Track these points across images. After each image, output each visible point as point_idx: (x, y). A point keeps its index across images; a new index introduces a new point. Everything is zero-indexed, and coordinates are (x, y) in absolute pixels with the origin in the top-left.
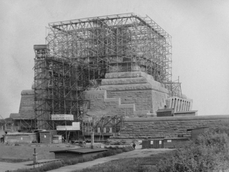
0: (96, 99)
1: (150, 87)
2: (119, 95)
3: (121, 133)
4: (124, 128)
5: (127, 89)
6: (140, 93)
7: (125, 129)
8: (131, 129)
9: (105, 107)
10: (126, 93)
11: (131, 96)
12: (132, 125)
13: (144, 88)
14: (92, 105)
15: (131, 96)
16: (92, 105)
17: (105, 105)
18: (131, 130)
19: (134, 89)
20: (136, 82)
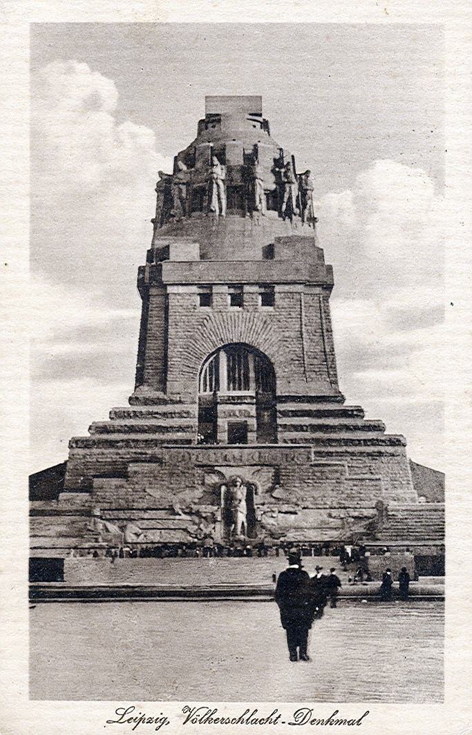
14: (283, 476)
16: (283, 476)
18: (404, 529)
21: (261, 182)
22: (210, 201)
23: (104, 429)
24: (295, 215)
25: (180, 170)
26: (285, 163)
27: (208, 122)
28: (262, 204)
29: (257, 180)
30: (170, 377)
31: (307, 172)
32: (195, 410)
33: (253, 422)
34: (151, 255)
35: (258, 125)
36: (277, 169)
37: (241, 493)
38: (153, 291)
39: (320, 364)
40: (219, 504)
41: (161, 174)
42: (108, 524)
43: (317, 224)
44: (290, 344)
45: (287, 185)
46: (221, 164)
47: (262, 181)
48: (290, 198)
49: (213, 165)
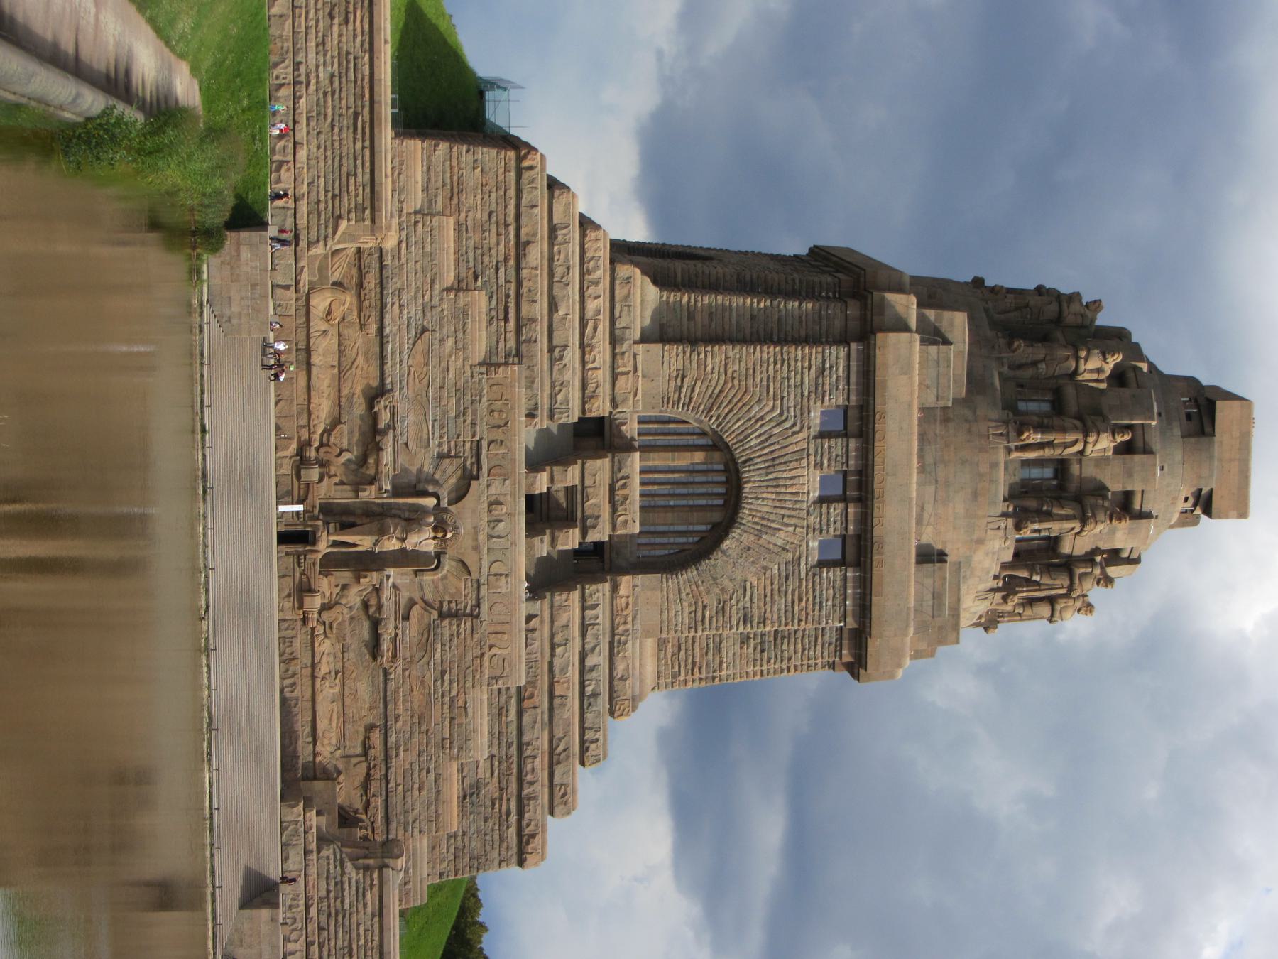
0: (486, 648)
1: (530, 859)
2: (500, 714)
3: (328, 858)
4: (353, 875)
6: (508, 813)
7: (350, 879)
8: (347, 907)
9: (447, 699)
10: (509, 745)
11: (492, 774)
12: (365, 906)
13: (527, 831)
14: (458, 626)
15: (496, 773)
17: (454, 693)
19: (525, 785)
20: (558, 771)
21: (1077, 530)
22: (1041, 428)
24: (1005, 599)
25: (1105, 359)
26: (1112, 571)
29: (1077, 525)
30: (673, 351)
31: (1089, 608)
32: (601, 408)
33: (570, 540)
35: (1188, 506)
36: (1098, 559)
37: (423, 540)
38: (853, 310)
39: (694, 663)
41: (1096, 305)
43: (981, 629)
44: (738, 601)
45: (1066, 583)
46: (1115, 447)
47: (1078, 534)
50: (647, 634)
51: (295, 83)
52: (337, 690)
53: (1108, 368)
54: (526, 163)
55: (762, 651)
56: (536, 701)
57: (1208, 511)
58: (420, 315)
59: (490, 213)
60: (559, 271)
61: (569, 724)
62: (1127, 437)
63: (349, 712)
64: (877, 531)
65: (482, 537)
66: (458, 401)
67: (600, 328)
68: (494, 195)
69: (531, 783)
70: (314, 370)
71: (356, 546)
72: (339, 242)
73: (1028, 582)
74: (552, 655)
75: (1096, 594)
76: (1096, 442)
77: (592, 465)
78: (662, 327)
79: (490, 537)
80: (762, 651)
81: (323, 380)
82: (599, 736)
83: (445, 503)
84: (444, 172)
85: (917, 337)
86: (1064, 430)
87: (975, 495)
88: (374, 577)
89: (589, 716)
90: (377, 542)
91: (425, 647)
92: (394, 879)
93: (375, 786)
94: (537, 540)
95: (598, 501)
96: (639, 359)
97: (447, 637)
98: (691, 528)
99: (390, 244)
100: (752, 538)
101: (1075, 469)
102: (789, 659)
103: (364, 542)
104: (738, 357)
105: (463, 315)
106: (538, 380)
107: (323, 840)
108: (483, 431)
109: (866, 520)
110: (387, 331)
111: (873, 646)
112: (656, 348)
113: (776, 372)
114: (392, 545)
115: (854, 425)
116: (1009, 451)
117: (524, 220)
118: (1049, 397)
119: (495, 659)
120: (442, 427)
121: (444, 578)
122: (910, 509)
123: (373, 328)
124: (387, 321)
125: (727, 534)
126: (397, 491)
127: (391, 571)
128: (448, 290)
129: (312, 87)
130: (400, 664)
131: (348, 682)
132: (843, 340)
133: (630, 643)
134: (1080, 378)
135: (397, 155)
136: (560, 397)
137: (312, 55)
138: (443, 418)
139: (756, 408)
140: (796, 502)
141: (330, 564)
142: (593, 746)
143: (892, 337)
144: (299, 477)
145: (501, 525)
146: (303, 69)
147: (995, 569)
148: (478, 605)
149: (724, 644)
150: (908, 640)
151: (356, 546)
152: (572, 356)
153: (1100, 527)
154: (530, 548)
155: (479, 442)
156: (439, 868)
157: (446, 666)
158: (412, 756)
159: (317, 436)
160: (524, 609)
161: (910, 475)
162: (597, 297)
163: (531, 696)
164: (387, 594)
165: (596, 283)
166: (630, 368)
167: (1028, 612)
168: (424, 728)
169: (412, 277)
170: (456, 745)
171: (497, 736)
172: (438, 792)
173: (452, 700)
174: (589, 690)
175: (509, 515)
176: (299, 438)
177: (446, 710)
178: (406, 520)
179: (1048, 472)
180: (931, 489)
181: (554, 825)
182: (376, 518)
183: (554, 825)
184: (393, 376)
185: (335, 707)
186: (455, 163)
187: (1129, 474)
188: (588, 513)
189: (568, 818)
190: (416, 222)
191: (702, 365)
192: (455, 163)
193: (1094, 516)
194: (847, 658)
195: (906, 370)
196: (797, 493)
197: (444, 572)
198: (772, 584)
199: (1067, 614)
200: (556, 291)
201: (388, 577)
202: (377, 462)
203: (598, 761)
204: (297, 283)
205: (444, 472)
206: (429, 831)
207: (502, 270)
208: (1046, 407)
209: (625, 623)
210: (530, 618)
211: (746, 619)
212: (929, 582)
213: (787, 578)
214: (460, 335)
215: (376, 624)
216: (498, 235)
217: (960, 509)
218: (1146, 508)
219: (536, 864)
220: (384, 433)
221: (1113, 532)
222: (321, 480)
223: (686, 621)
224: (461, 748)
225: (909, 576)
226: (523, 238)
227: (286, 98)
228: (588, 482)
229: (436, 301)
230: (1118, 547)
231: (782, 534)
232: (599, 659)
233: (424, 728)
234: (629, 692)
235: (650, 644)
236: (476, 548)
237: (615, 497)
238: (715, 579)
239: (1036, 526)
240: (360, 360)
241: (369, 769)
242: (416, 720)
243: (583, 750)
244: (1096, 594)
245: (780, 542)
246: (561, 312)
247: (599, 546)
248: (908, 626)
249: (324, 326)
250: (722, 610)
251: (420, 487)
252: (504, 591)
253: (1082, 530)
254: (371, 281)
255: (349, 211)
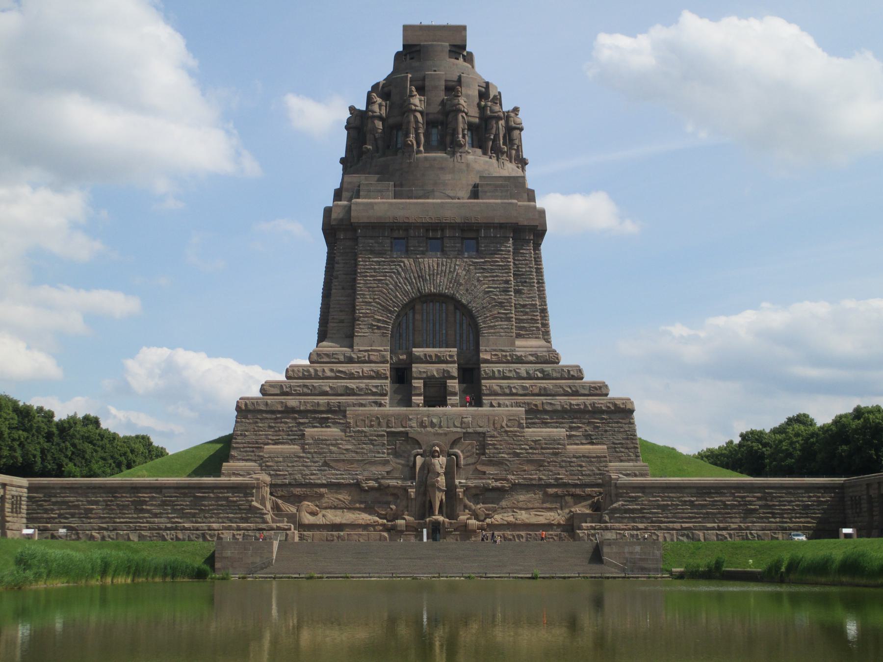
4: (620, 503)
5: (568, 407)
8: (639, 507)
11: (580, 427)
17: (527, 447)
20: (582, 391)
21: (464, 115)
22: (407, 135)
23: (281, 390)
26: (491, 97)
27: (406, 55)
28: (464, 137)
31: (516, 110)
32: (385, 368)
33: (454, 385)
34: (338, 195)
35: (461, 59)
36: (483, 103)
40: (415, 479)
42: (280, 501)
44: (496, 295)
47: (466, 114)
48: (497, 135)
49: (412, 96)
50: (513, 344)
51: (176, 529)
52: (523, 512)
53: (379, 100)
54: (243, 407)
55: (525, 282)
56: (538, 403)
57: (464, 47)
58: (317, 464)
59: (270, 427)
60: (305, 390)
61: (556, 386)
62: (413, 88)
63: (537, 505)
64: (458, 221)
65: (440, 431)
66: (364, 444)
67: (341, 369)
68: (260, 425)
69: (585, 405)
70: (344, 521)
71: (442, 500)
72: (265, 507)
73: (494, 141)
74: (516, 394)
75: (507, 106)
76: (416, 106)
77: (414, 375)
78: (347, 337)
79: (440, 427)
80: (525, 282)
81: (349, 517)
82: (565, 369)
83: (420, 451)
84: (246, 451)
85: (354, 201)
86: (409, 122)
87: (442, 169)
88: (460, 491)
89: (555, 375)
90: (440, 490)
91: (499, 463)
92: (625, 479)
93: (578, 491)
94: (449, 402)
95: (434, 369)
96: (362, 348)
97: (496, 451)
98: (458, 321)
99: (268, 479)
100: (461, 288)
101: (431, 117)
102: (530, 267)
103: (440, 497)
104: (364, 295)
105: (318, 441)
106: (361, 401)
107: (601, 521)
108: (382, 430)
109: (453, 226)
110: (324, 482)
111: (523, 222)
112: (356, 340)
113: (371, 276)
114: (442, 480)
115: (401, 233)
116: (419, 152)
117: (274, 408)
118: (395, 132)
119: (509, 424)
120: (379, 453)
121: (462, 451)
122: (446, 203)
123: (323, 490)
124: (319, 482)
125: (459, 302)
126: (413, 478)
127: (457, 482)
128: (303, 449)
129: (179, 520)
130: (509, 477)
131: (520, 505)
132: (355, 240)
133: (519, 354)
134: (384, 115)
135: (229, 475)
136: (374, 390)
137: (162, 520)
138: (373, 452)
139: (391, 286)
140: (443, 265)
141: (452, 515)
142: (572, 373)
143: (353, 214)
144: (402, 532)
145: (435, 420)
146: (169, 525)
147: (486, 158)
148: (479, 433)
149: (521, 303)
150: (519, 203)
151: (442, 500)
152: (352, 384)
153: (462, 102)
154: (453, 405)
155: (388, 432)
156: (633, 457)
157: (511, 451)
158: (563, 471)
159: (380, 521)
160: (485, 409)
161: (428, 203)
162: (324, 371)
163: (536, 405)
164: (471, 483)
165: (316, 371)
166: (366, 354)
167: (517, 142)
168: (546, 464)
169: (296, 468)
170: (556, 446)
171: (558, 425)
172: (584, 456)
173: (531, 448)
174: (540, 375)
175: (428, 417)
176: (380, 531)
177: (537, 451)
178: (428, 472)
179: (435, 133)
180: (437, 194)
181: (612, 394)
182: (426, 488)
183: (612, 394)
184: (349, 478)
185: (533, 513)
186: (242, 445)
187: (436, 88)
188: (441, 375)
189: (610, 387)
190: (267, 466)
191: (366, 315)
192: (242, 445)
193: (456, 105)
194: (532, 237)
195: (372, 204)
196: (438, 264)
197: (459, 452)
198: (487, 277)
199: (518, 121)
200: (317, 392)
201: (460, 483)
202: (395, 487)
203: (580, 371)
204: (285, 529)
205: (404, 452)
206: (606, 461)
207: (301, 421)
208: (400, 133)
209: (506, 356)
210: (492, 406)
211: (506, 291)
212: (488, 194)
213: (484, 269)
214: (329, 442)
215: (486, 489)
216: (281, 422)
217: (448, 177)
218: (455, 78)
219: (632, 403)
220: (380, 485)
221: (468, 96)
222: (404, 519)
223: (506, 323)
224: (559, 444)
225: (484, 203)
226: (283, 409)
227: (184, 534)
228: (424, 375)
229: (309, 456)
230: (477, 93)
231: (460, 271)
232: (522, 369)
233: (546, 464)
234: (544, 354)
235: (519, 342)
236: (446, 434)
237: (436, 360)
238: (484, 308)
239: (460, 136)
240: (340, 497)
241: (569, 495)
242: (541, 469)
243: (573, 378)
244: (507, 106)
245: (464, 273)
246: (328, 389)
247: (459, 369)
248: (511, 203)
249: (320, 515)
250: (501, 304)
251: (411, 464)
252: (470, 419)
253: (464, 112)
254: (297, 491)
255: (247, 501)
